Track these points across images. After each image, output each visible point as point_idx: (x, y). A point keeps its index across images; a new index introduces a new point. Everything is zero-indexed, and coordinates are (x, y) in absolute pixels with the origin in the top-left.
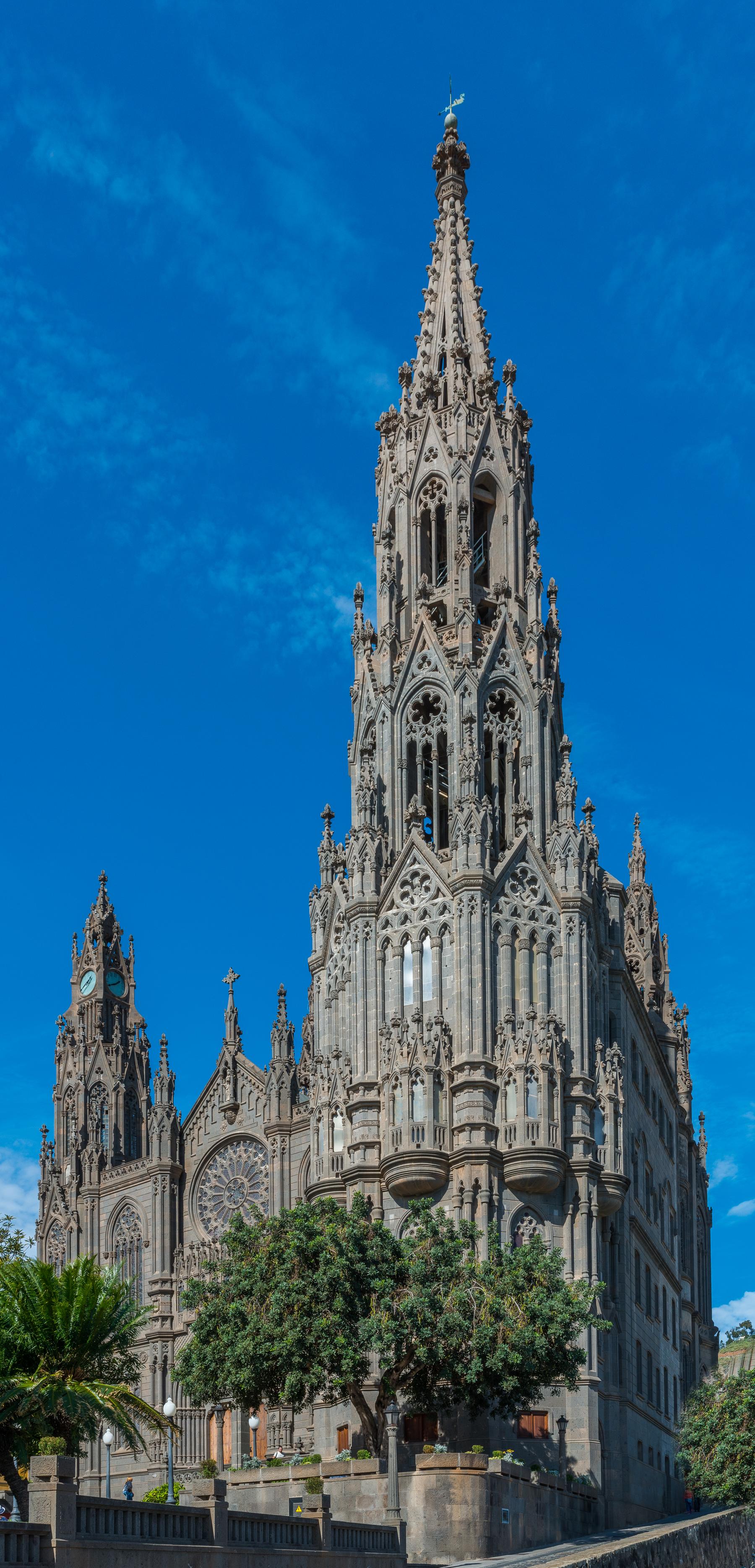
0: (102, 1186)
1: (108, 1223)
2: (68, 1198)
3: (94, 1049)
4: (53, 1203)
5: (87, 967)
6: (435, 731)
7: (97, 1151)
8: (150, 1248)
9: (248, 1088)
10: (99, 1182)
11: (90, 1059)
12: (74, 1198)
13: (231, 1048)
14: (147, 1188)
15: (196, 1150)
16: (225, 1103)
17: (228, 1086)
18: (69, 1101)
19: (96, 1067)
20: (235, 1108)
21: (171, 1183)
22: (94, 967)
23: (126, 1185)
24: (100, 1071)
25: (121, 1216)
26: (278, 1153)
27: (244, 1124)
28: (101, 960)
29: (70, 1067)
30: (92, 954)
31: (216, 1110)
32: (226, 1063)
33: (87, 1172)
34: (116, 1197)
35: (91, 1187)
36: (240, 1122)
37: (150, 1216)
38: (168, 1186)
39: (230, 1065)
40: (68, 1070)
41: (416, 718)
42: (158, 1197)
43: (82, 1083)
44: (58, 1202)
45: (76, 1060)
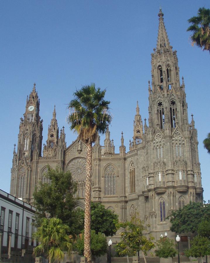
6: (161, 108)
15: (68, 158)
25: (45, 169)
26: (98, 165)
41: (158, 106)
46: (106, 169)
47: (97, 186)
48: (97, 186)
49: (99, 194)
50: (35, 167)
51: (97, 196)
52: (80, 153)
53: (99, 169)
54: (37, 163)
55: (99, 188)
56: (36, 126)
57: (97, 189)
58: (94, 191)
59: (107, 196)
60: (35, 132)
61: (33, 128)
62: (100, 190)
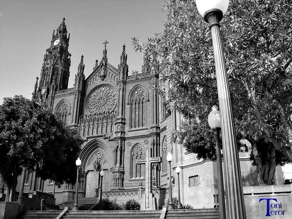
0: (56, 95)
1: (56, 107)
2: (43, 98)
3: (57, 58)
4: (37, 99)
5: (57, 38)
7: (56, 84)
8: (71, 115)
9: (109, 71)
10: (55, 94)
11: (55, 61)
12: (45, 98)
13: (105, 60)
14: (73, 97)
16: (101, 75)
17: (103, 70)
18: (46, 71)
19: (57, 63)
20: (105, 76)
21: (81, 96)
22: (60, 38)
23: (64, 95)
24: (57, 64)
27: (107, 81)
28: (62, 36)
29: (49, 62)
30: (59, 35)
31: (97, 77)
32: (103, 64)
33: (51, 91)
34: (60, 99)
35: (52, 95)
36: (106, 80)
37: (72, 105)
38: (80, 97)
39: (104, 64)
40: (48, 63)
42: (76, 100)
43: (52, 66)
44: (39, 99)
45: (51, 60)
46: (132, 93)
47: (120, 116)
48: (120, 116)
49: (122, 127)
50: (50, 103)
51: (119, 130)
52: (103, 80)
53: (124, 94)
54: (53, 98)
55: (122, 119)
56: (59, 59)
57: (120, 121)
58: (116, 124)
59: (133, 129)
60: (56, 66)
61: (54, 61)
62: (123, 121)
